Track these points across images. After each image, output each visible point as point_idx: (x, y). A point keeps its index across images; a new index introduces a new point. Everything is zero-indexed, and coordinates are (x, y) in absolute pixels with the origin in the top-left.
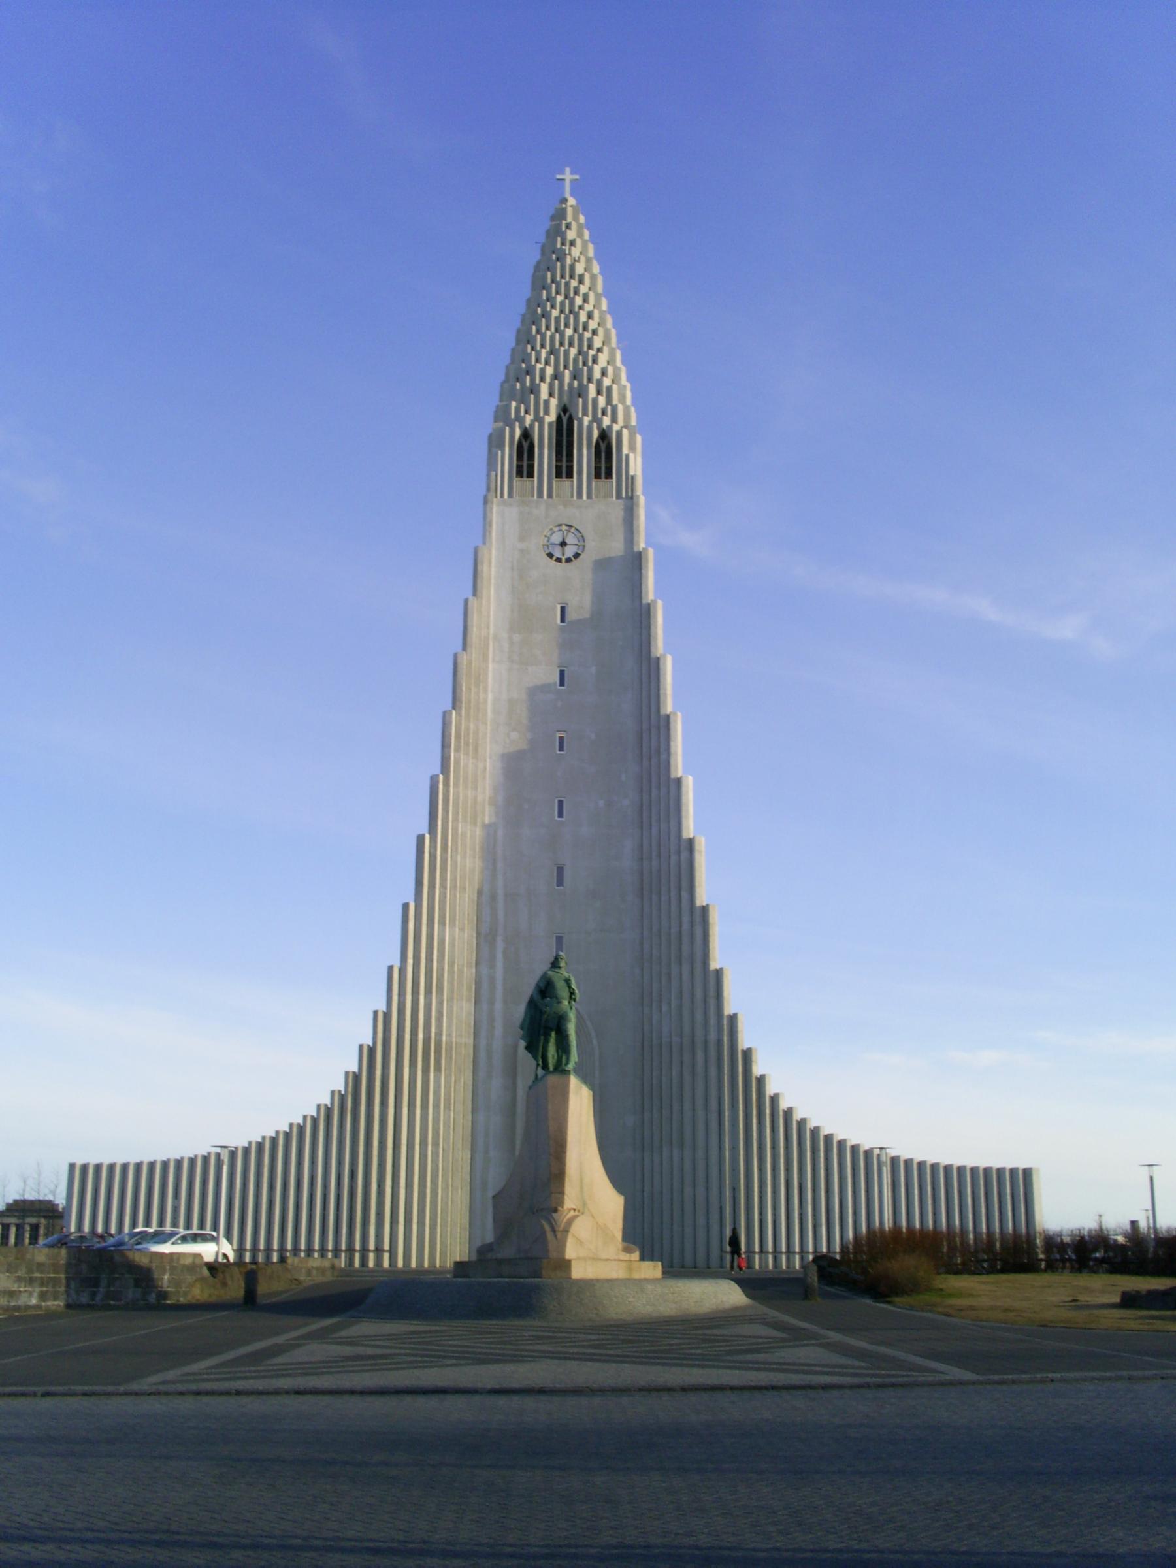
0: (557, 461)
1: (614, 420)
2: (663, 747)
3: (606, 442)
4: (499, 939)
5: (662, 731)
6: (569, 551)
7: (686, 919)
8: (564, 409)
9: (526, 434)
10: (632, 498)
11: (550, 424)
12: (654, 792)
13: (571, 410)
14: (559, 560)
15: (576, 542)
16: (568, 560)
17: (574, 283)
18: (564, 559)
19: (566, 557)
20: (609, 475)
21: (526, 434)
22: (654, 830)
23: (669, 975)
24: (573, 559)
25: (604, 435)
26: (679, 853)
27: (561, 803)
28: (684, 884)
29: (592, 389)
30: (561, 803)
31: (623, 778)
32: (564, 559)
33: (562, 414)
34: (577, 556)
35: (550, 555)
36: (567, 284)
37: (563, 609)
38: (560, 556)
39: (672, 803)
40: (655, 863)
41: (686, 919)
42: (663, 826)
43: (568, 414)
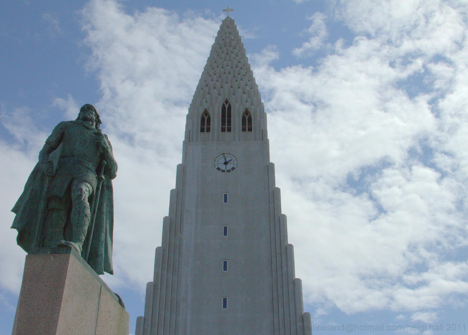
0: (222, 125)
1: (252, 104)
2: (284, 264)
3: (248, 116)
6: (229, 167)
8: (227, 102)
9: (206, 113)
10: (263, 140)
14: (223, 171)
16: (229, 171)
18: (226, 171)
19: (228, 169)
20: (250, 130)
21: (206, 113)
24: (231, 170)
25: (247, 112)
27: (225, 300)
30: (225, 300)
32: (226, 171)
33: (225, 104)
34: (233, 169)
35: (219, 169)
36: (227, 49)
37: (226, 196)
38: (224, 169)
43: (228, 104)
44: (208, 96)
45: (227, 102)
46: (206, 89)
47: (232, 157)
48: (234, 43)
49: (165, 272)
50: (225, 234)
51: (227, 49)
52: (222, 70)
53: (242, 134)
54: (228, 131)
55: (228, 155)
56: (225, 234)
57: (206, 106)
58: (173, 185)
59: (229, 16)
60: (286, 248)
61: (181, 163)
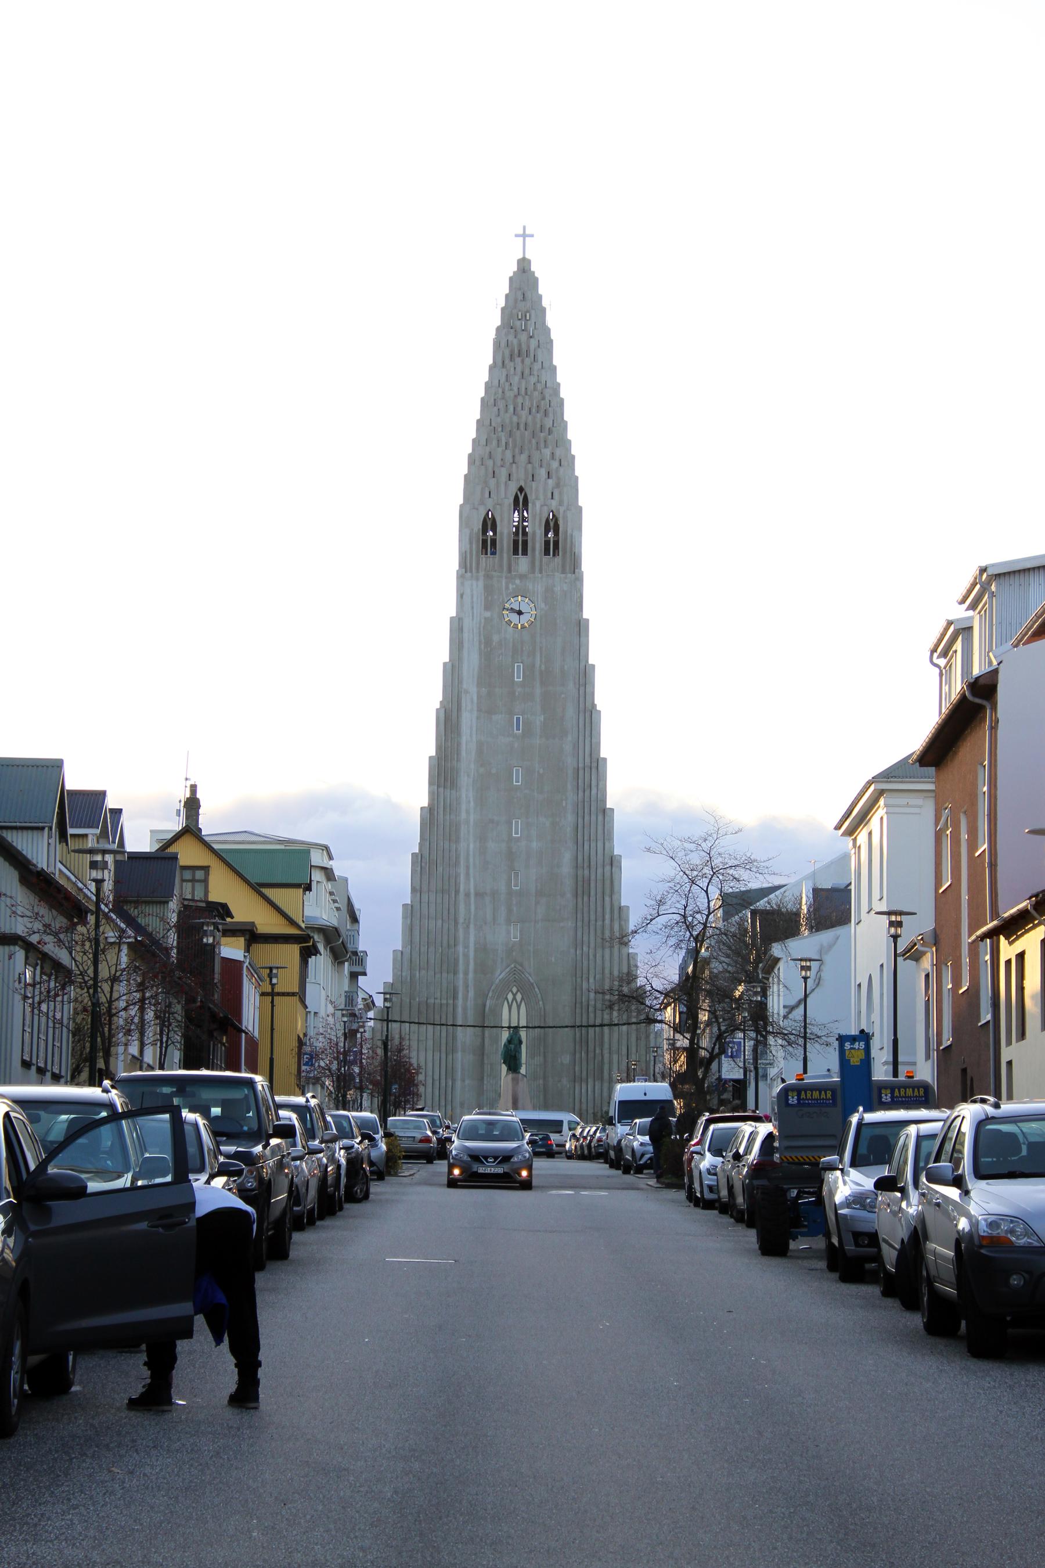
1: (561, 503)
4: (472, 926)
5: (594, 771)
7: (607, 916)
8: (521, 489)
10: (574, 573)
11: (510, 505)
12: (587, 818)
13: (527, 490)
15: (530, 611)
17: (528, 361)
18: (519, 628)
19: (521, 623)
22: (586, 847)
23: (595, 956)
26: (604, 866)
28: (608, 891)
29: (543, 472)
31: (564, 804)
32: (519, 628)
33: (519, 493)
36: (523, 362)
38: (517, 622)
39: (600, 828)
40: (586, 872)
41: (607, 916)
42: (593, 845)
43: (523, 494)
44: (492, 482)
45: (521, 489)
46: (490, 463)
47: (530, 602)
48: (533, 343)
49: (441, 790)
50: (518, 729)
51: (523, 362)
52: (515, 419)
53: (545, 559)
54: (522, 555)
55: (523, 599)
56: (518, 729)
57: (490, 503)
58: (444, 655)
59: (527, 256)
60: (598, 760)
61: (454, 615)
